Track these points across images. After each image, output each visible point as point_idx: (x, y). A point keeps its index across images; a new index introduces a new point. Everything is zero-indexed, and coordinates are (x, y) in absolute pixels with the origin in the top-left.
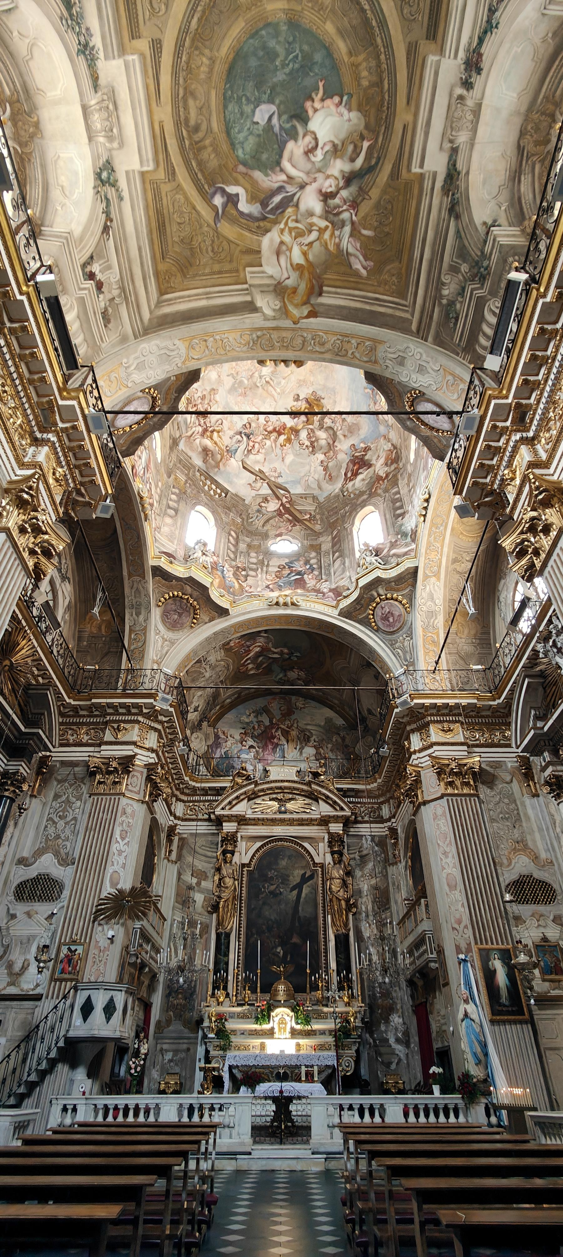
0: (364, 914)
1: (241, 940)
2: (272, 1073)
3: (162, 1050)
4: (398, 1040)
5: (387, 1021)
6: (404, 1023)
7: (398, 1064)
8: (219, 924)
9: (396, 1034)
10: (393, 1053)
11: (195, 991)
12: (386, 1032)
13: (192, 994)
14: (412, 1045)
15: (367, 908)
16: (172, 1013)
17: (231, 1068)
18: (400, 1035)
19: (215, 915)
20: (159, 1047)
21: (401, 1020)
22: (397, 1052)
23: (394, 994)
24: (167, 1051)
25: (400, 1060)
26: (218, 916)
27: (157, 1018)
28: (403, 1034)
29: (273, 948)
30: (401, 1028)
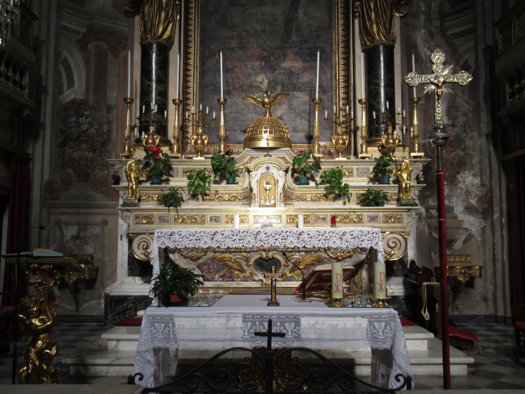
0: (422, 17)
1: (191, 62)
2: (247, 260)
3: (58, 223)
4: (469, 209)
5: (453, 181)
6: (483, 185)
7: (465, 242)
8: (148, 29)
9: (466, 200)
10: (459, 226)
11: (109, 139)
12: (450, 197)
13: (105, 144)
14: (496, 216)
15: (429, 7)
16: (71, 171)
17: (165, 252)
18: (473, 202)
19: (137, 19)
20: (53, 219)
21: (477, 181)
22: (466, 225)
23: (469, 143)
24: (68, 224)
25: (470, 237)
26: (143, 18)
27: (46, 177)
28: (480, 200)
29: (250, 75)
30: (476, 191)
